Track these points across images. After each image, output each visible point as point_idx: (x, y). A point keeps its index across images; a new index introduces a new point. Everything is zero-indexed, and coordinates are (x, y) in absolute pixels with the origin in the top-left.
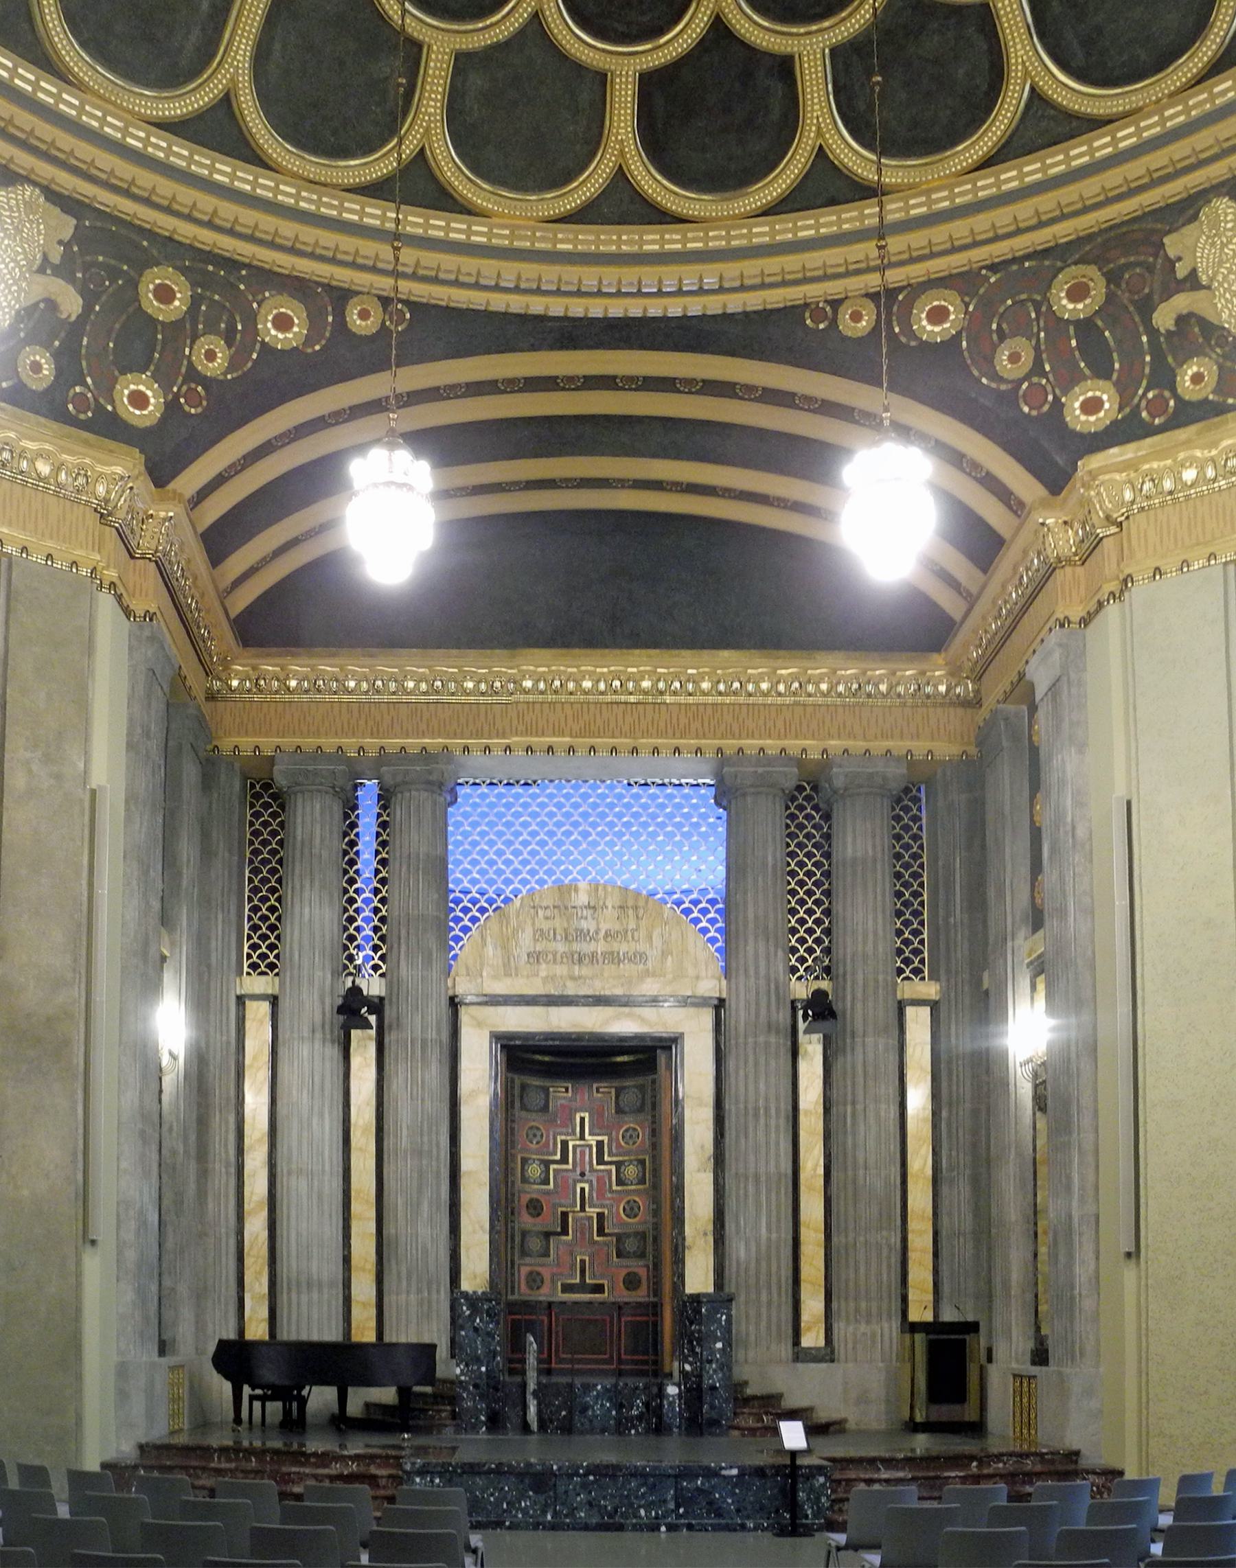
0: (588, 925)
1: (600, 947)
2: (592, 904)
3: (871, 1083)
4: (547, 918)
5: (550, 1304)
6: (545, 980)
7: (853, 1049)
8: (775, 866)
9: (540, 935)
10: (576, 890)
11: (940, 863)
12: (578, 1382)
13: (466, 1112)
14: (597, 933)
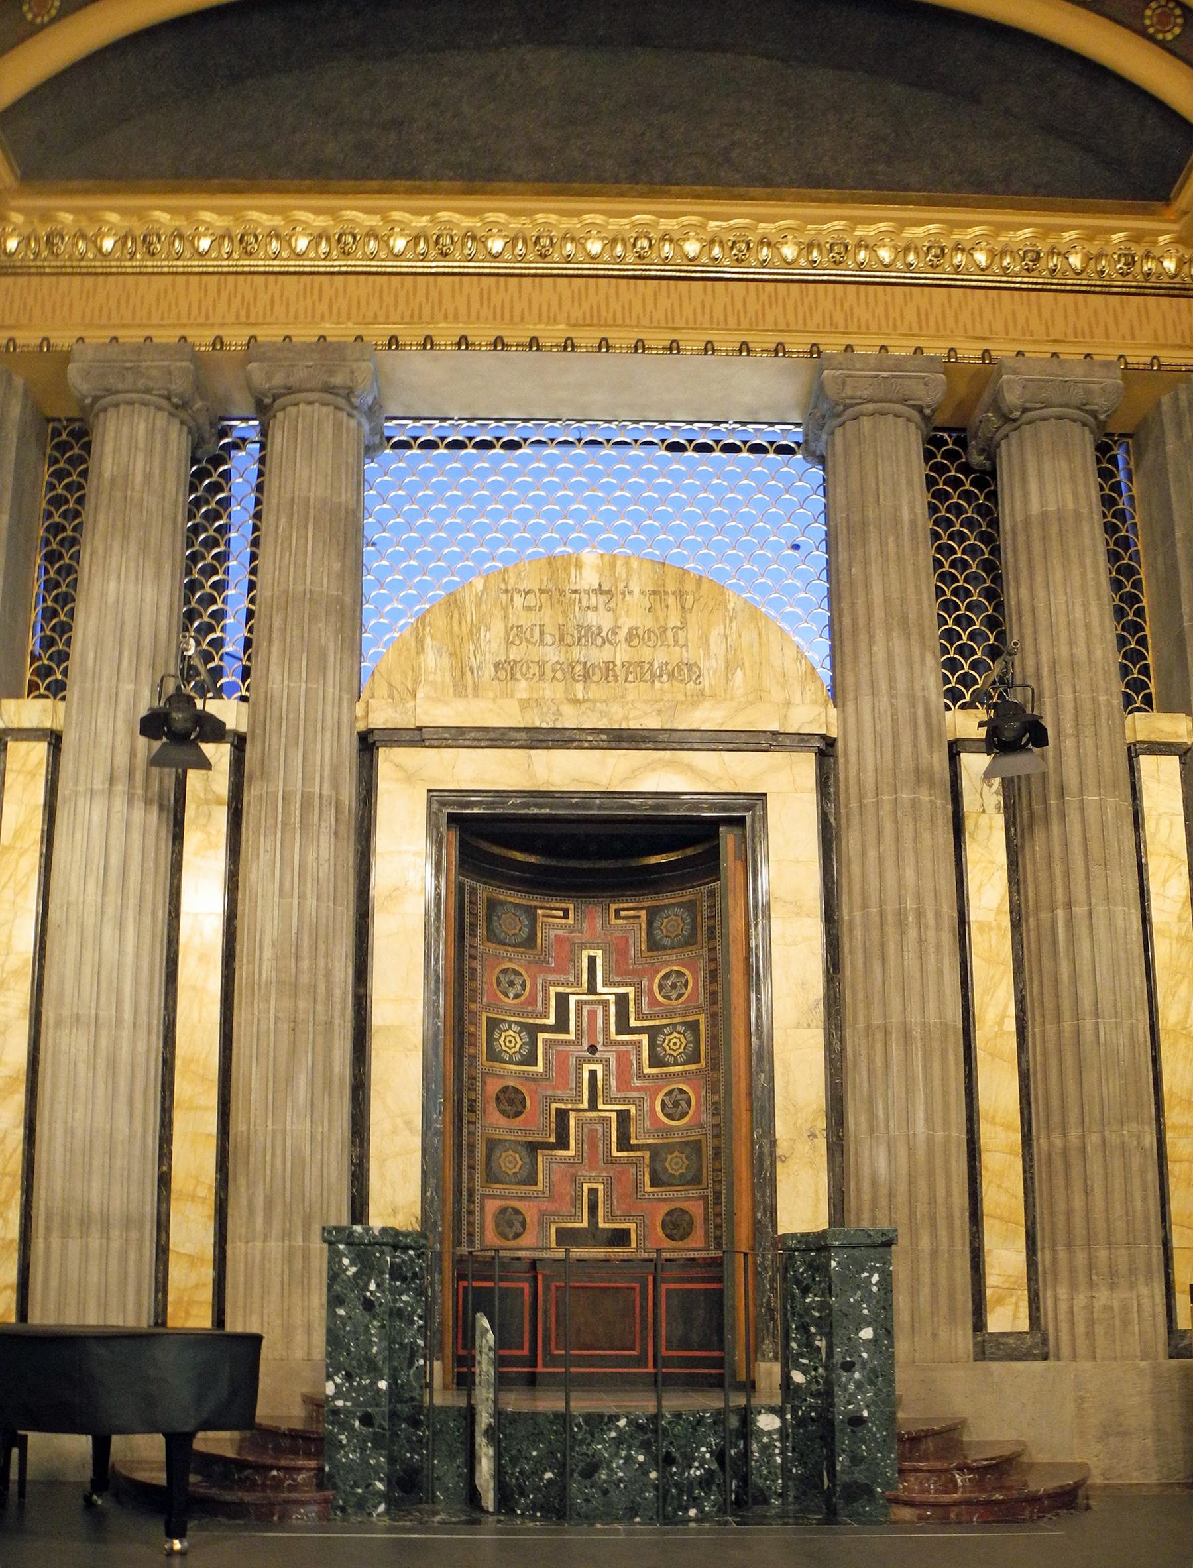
0: (599, 619)
1: (622, 654)
2: (605, 588)
3: (1096, 870)
4: (529, 609)
5: (534, 1263)
6: (524, 705)
7: (1063, 815)
8: (913, 523)
9: (514, 634)
10: (579, 566)
11: (1178, 535)
12: (582, 1404)
13: (382, 926)
14: (615, 633)
